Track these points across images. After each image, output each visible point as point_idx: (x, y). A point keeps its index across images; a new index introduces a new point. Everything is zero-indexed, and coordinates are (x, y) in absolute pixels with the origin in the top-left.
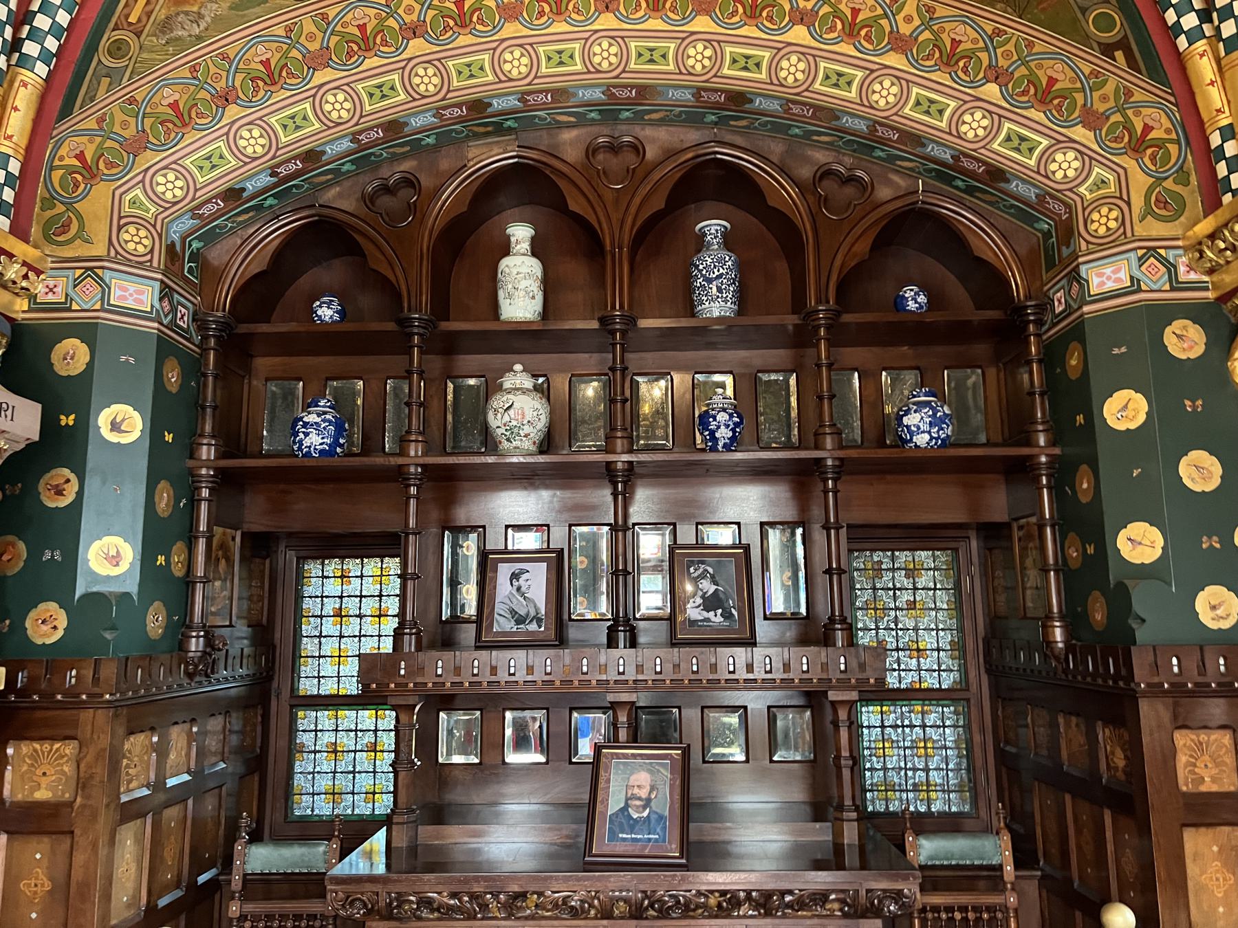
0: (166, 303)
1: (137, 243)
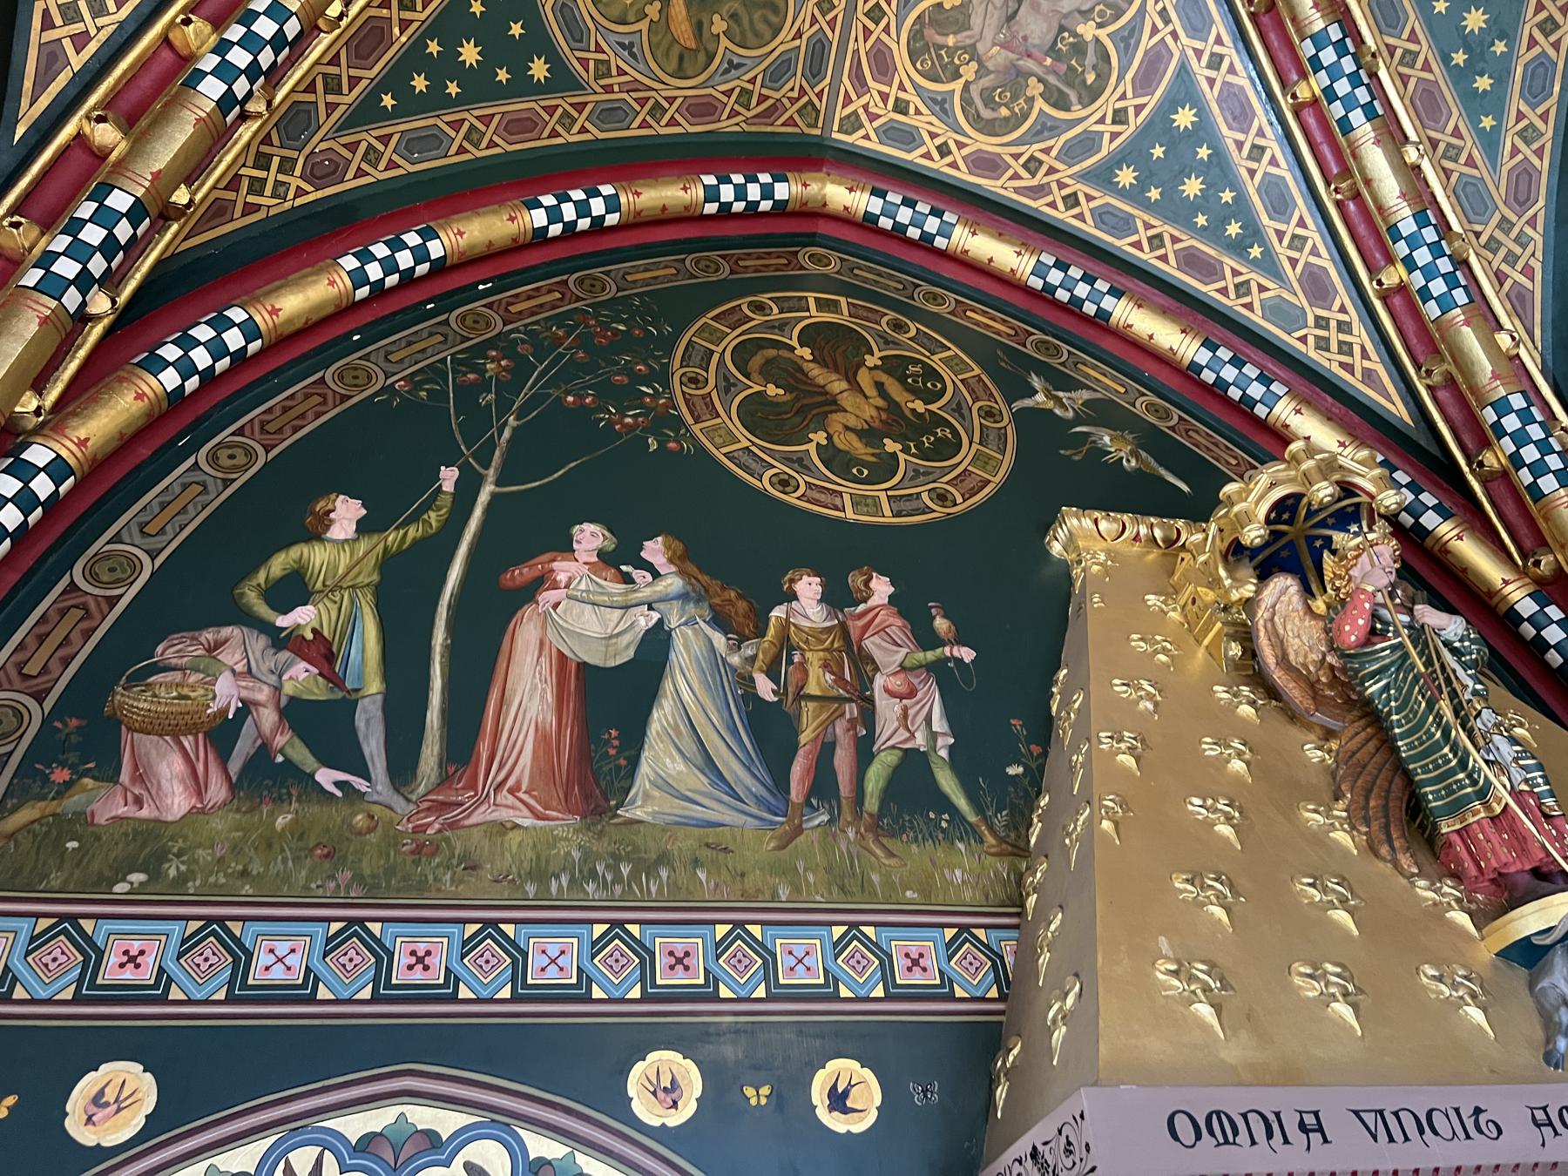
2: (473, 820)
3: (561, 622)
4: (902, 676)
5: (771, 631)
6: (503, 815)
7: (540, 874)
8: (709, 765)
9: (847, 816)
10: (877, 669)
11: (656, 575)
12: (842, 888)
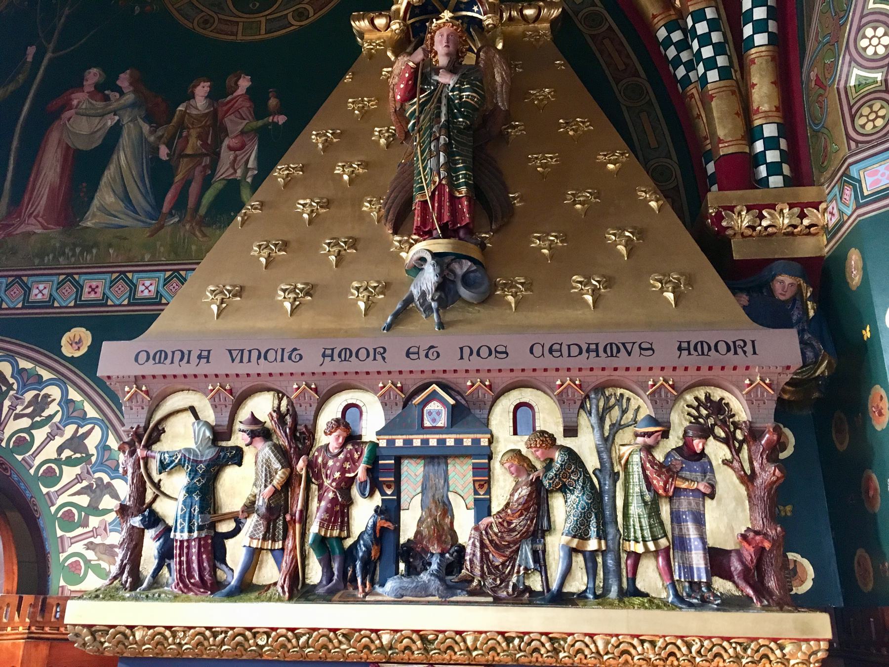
1: (873, 121)
2: (18, 231)
3: (71, 128)
4: (239, 137)
5: (175, 119)
6: (30, 228)
7: (41, 255)
8: (126, 198)
9: (188, 218)
10: (227, 135)
11: (122, 93)
12: (176, 253)
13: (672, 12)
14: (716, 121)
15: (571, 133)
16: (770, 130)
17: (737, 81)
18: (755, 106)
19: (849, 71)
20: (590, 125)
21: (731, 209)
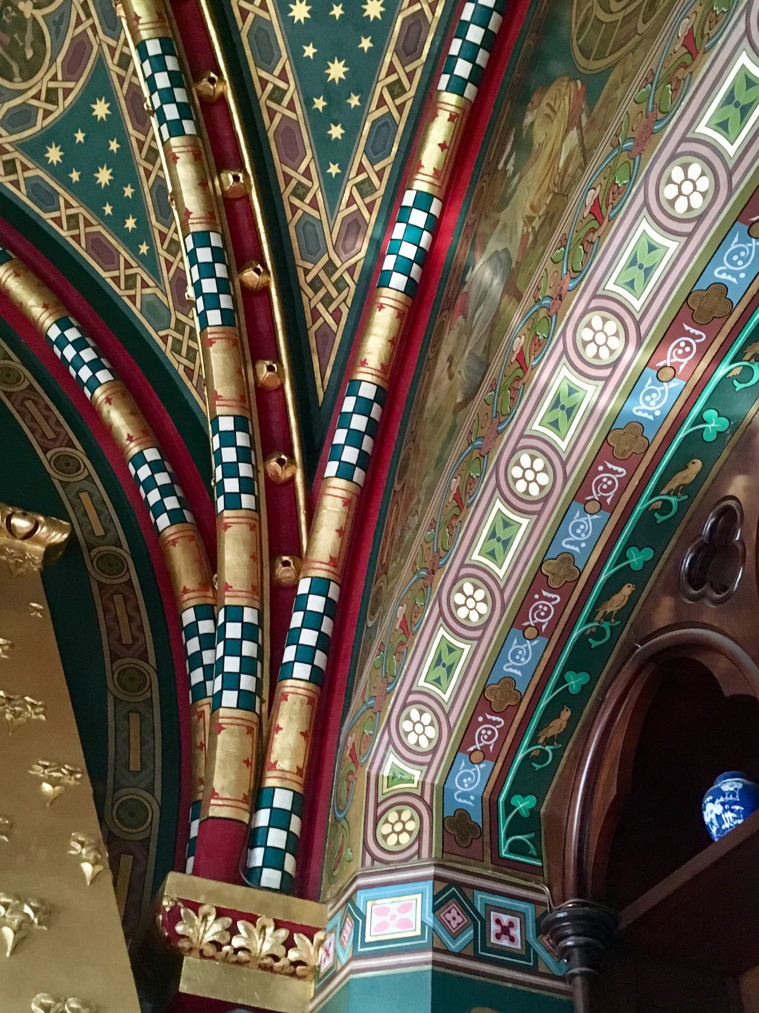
0: (454, 916)
1: (398, 833)
13: (210, 594)
14: (218, 763)
15: (8, 716)
16: (283, 800)
17: (260, 717)
18: (272, 760)
19: (384, 756)
20: (44, 713)
21: (195, 907)
